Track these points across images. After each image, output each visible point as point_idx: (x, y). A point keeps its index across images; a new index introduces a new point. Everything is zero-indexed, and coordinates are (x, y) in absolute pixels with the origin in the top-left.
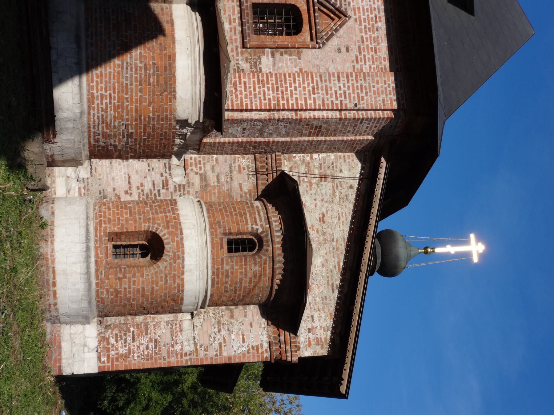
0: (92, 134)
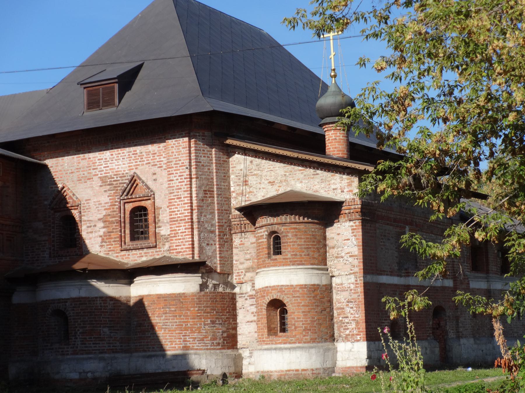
0: (212, 347)
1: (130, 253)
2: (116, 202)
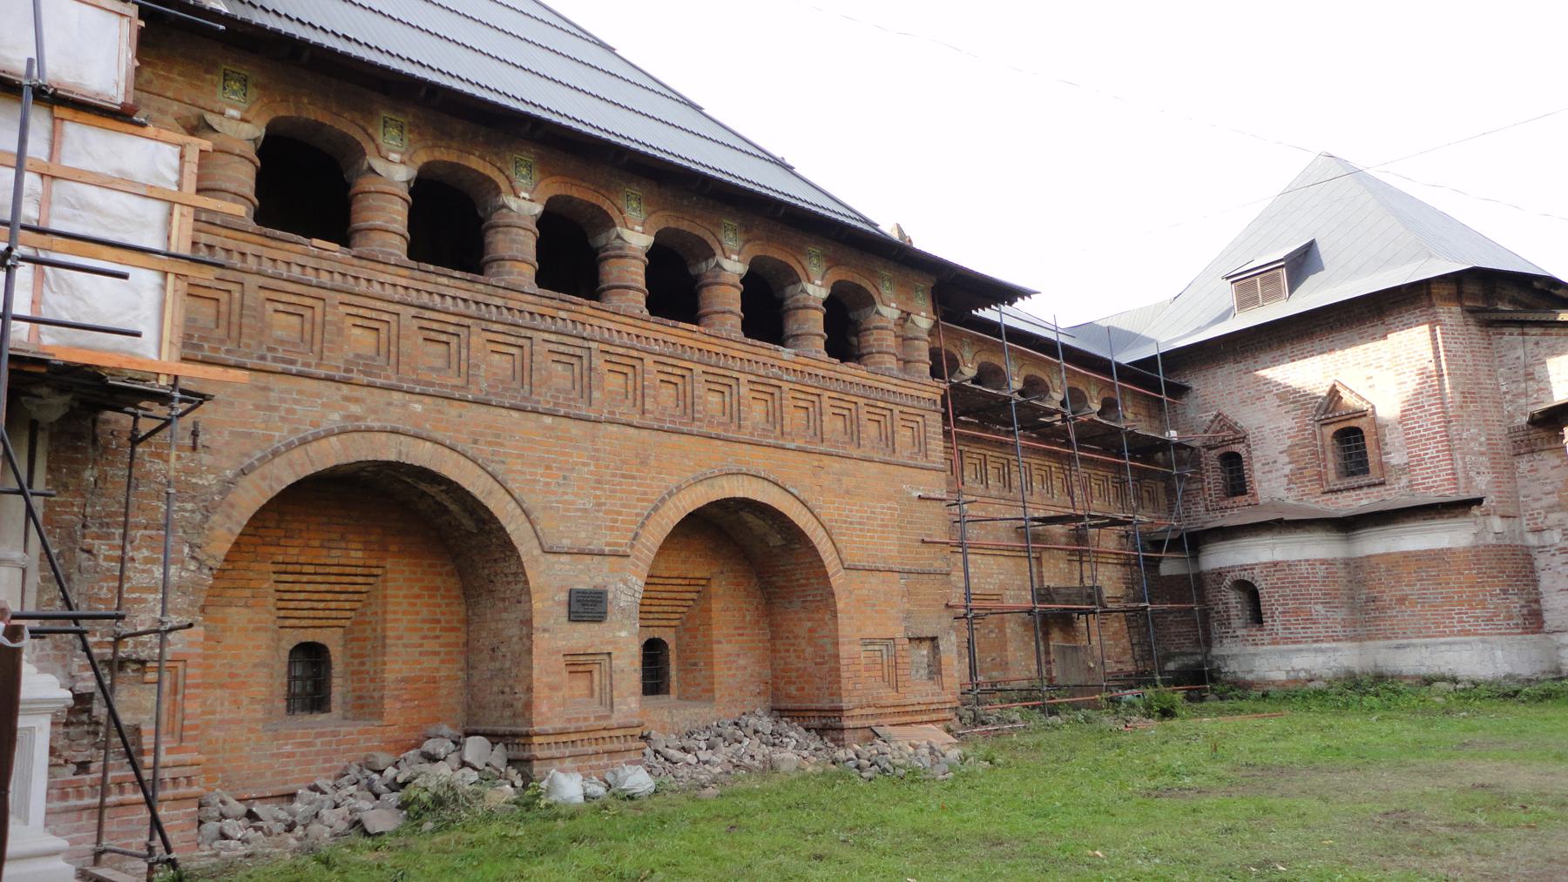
1: (1339, 495)
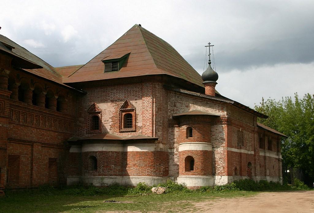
2: (118, 111)
